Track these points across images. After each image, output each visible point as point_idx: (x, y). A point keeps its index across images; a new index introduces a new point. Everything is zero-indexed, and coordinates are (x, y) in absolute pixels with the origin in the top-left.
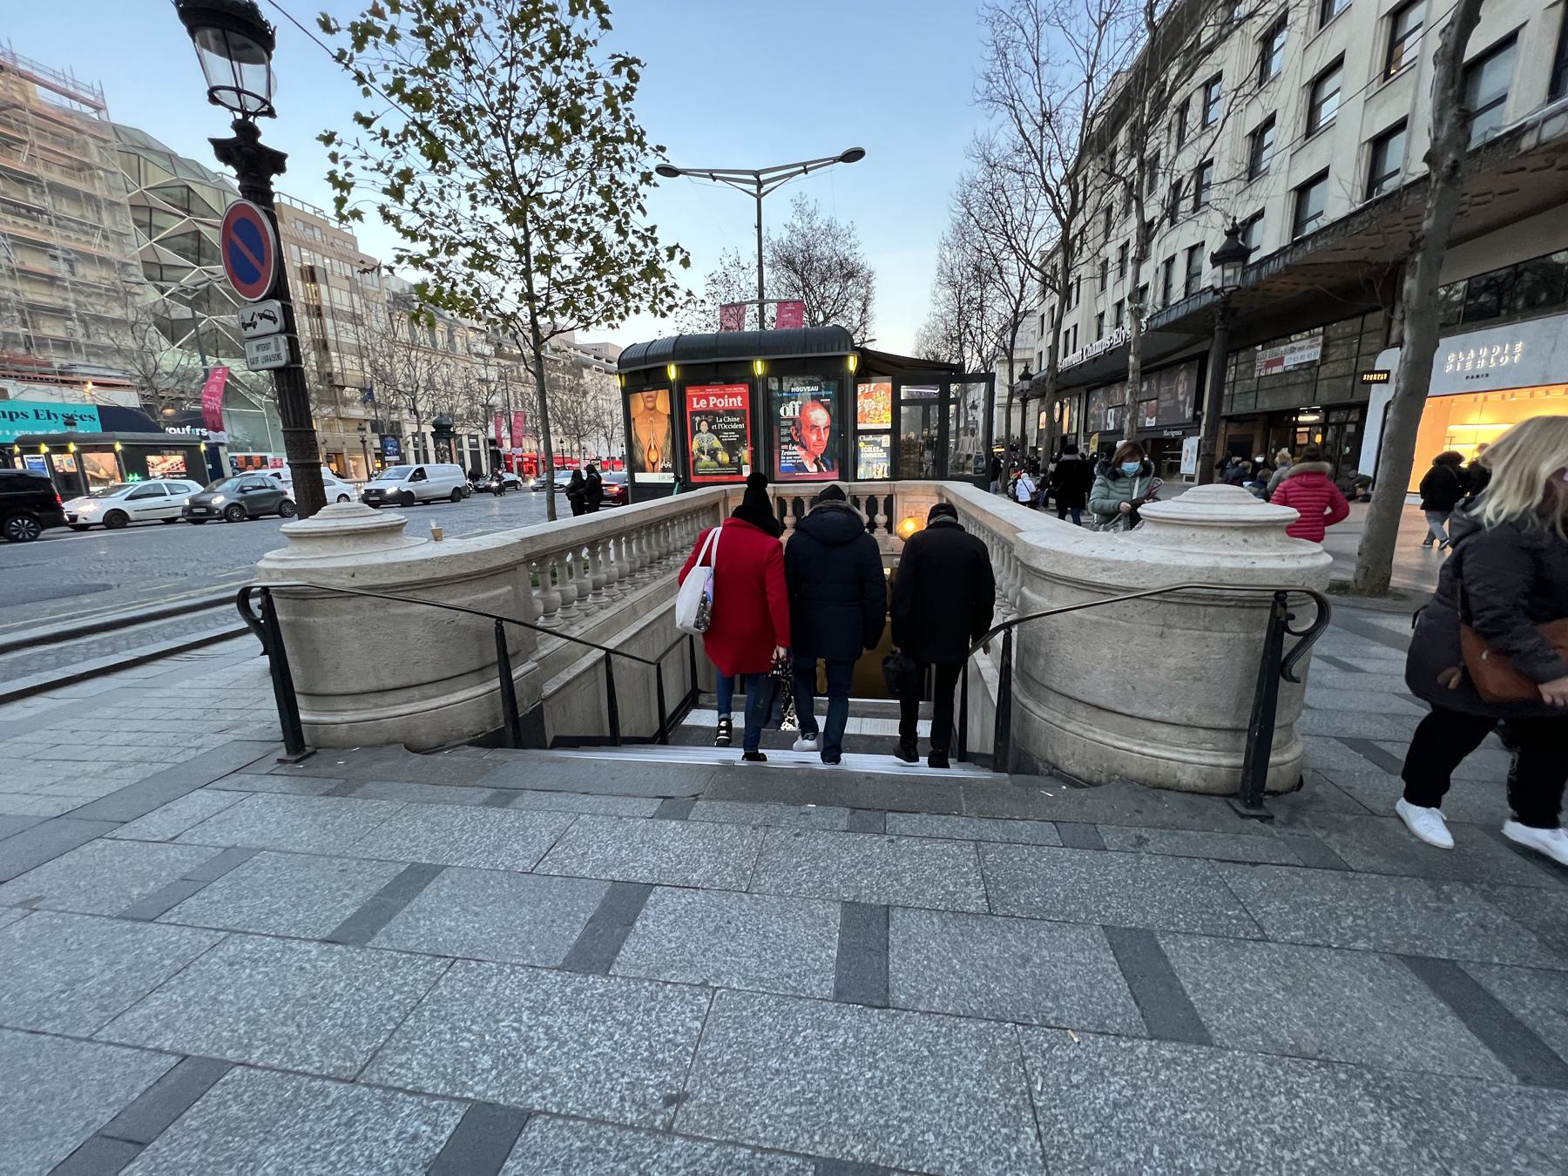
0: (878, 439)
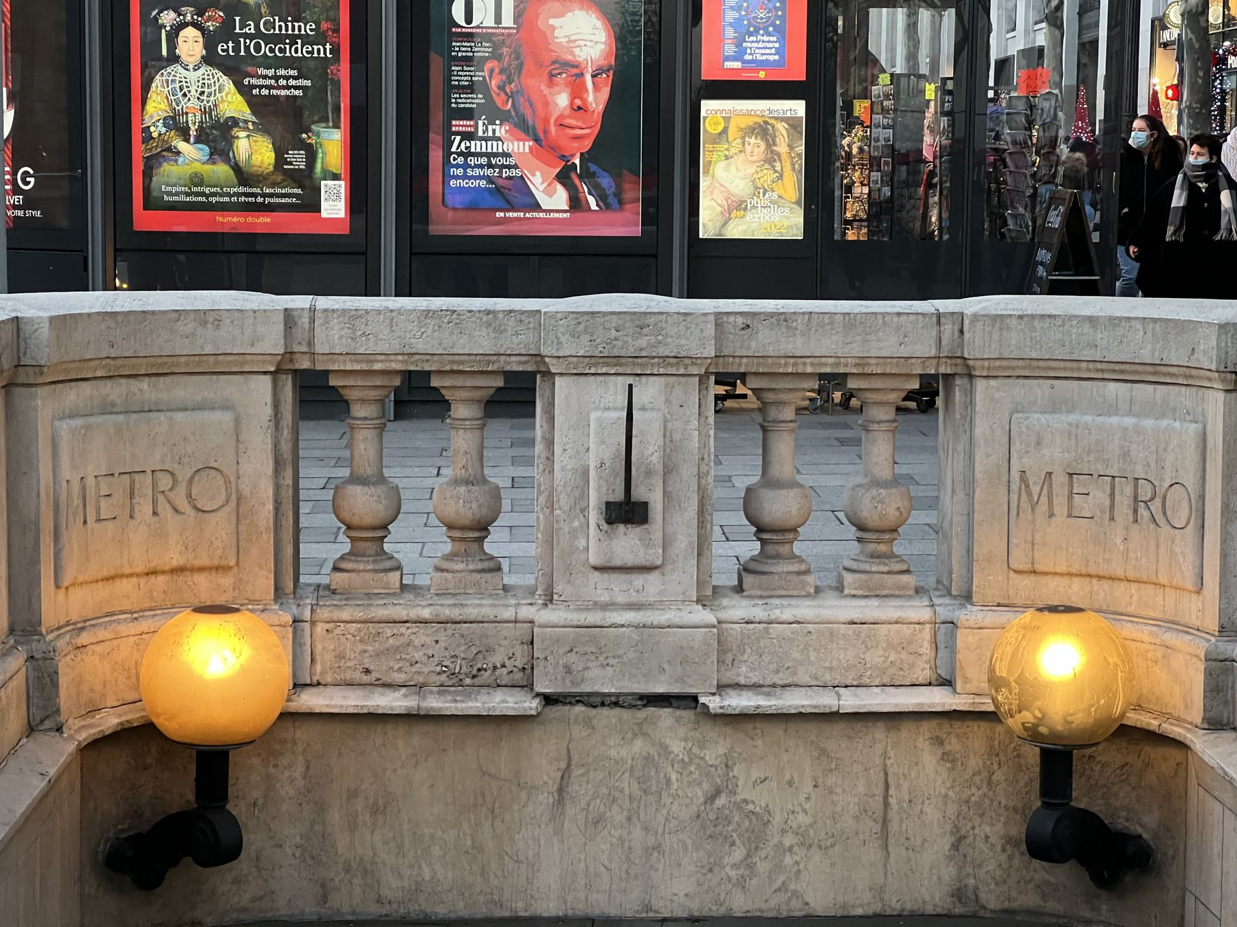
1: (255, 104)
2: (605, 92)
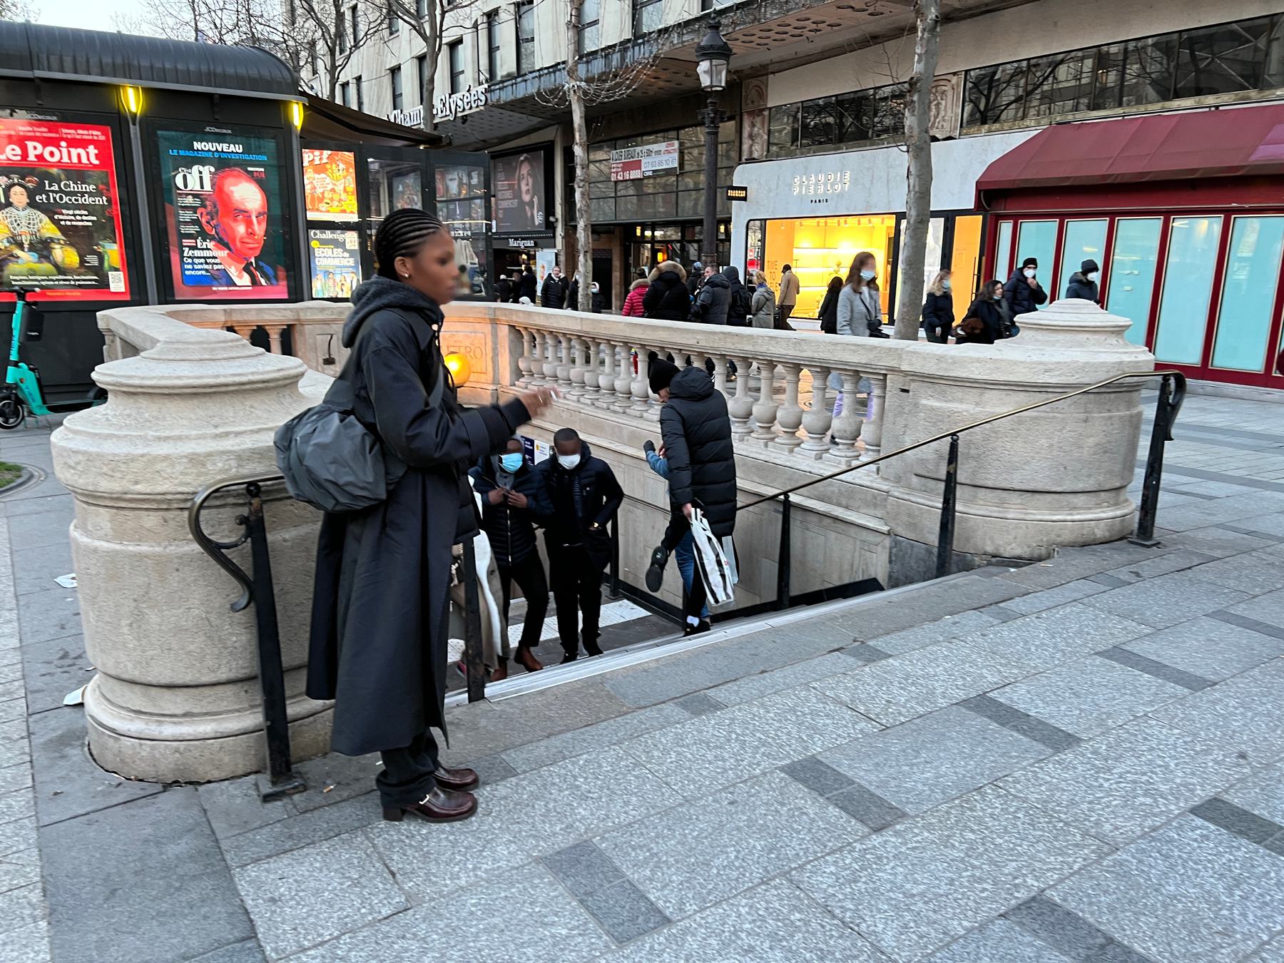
0: (338, 235)
1: (64, 230)
2: (264, 225)
